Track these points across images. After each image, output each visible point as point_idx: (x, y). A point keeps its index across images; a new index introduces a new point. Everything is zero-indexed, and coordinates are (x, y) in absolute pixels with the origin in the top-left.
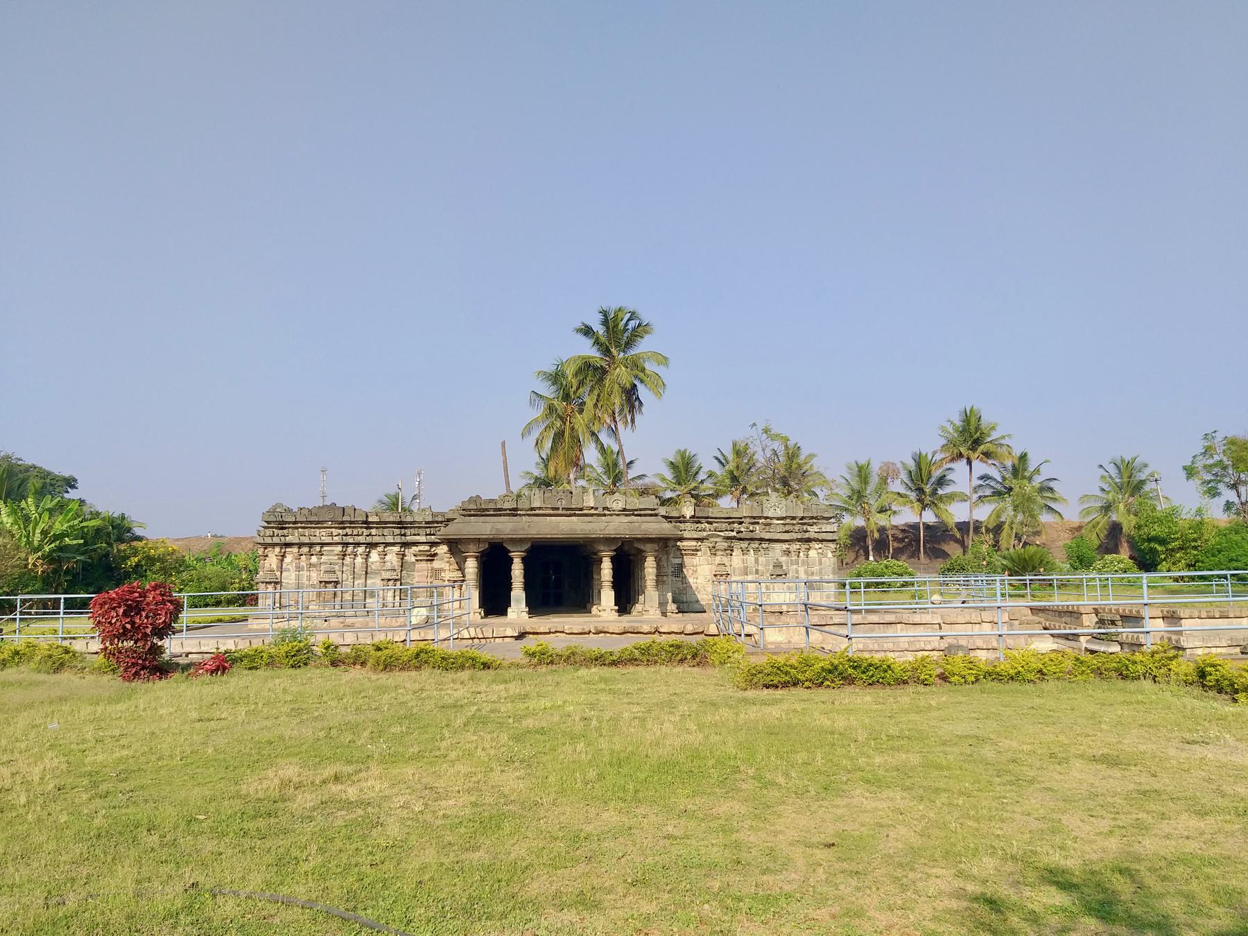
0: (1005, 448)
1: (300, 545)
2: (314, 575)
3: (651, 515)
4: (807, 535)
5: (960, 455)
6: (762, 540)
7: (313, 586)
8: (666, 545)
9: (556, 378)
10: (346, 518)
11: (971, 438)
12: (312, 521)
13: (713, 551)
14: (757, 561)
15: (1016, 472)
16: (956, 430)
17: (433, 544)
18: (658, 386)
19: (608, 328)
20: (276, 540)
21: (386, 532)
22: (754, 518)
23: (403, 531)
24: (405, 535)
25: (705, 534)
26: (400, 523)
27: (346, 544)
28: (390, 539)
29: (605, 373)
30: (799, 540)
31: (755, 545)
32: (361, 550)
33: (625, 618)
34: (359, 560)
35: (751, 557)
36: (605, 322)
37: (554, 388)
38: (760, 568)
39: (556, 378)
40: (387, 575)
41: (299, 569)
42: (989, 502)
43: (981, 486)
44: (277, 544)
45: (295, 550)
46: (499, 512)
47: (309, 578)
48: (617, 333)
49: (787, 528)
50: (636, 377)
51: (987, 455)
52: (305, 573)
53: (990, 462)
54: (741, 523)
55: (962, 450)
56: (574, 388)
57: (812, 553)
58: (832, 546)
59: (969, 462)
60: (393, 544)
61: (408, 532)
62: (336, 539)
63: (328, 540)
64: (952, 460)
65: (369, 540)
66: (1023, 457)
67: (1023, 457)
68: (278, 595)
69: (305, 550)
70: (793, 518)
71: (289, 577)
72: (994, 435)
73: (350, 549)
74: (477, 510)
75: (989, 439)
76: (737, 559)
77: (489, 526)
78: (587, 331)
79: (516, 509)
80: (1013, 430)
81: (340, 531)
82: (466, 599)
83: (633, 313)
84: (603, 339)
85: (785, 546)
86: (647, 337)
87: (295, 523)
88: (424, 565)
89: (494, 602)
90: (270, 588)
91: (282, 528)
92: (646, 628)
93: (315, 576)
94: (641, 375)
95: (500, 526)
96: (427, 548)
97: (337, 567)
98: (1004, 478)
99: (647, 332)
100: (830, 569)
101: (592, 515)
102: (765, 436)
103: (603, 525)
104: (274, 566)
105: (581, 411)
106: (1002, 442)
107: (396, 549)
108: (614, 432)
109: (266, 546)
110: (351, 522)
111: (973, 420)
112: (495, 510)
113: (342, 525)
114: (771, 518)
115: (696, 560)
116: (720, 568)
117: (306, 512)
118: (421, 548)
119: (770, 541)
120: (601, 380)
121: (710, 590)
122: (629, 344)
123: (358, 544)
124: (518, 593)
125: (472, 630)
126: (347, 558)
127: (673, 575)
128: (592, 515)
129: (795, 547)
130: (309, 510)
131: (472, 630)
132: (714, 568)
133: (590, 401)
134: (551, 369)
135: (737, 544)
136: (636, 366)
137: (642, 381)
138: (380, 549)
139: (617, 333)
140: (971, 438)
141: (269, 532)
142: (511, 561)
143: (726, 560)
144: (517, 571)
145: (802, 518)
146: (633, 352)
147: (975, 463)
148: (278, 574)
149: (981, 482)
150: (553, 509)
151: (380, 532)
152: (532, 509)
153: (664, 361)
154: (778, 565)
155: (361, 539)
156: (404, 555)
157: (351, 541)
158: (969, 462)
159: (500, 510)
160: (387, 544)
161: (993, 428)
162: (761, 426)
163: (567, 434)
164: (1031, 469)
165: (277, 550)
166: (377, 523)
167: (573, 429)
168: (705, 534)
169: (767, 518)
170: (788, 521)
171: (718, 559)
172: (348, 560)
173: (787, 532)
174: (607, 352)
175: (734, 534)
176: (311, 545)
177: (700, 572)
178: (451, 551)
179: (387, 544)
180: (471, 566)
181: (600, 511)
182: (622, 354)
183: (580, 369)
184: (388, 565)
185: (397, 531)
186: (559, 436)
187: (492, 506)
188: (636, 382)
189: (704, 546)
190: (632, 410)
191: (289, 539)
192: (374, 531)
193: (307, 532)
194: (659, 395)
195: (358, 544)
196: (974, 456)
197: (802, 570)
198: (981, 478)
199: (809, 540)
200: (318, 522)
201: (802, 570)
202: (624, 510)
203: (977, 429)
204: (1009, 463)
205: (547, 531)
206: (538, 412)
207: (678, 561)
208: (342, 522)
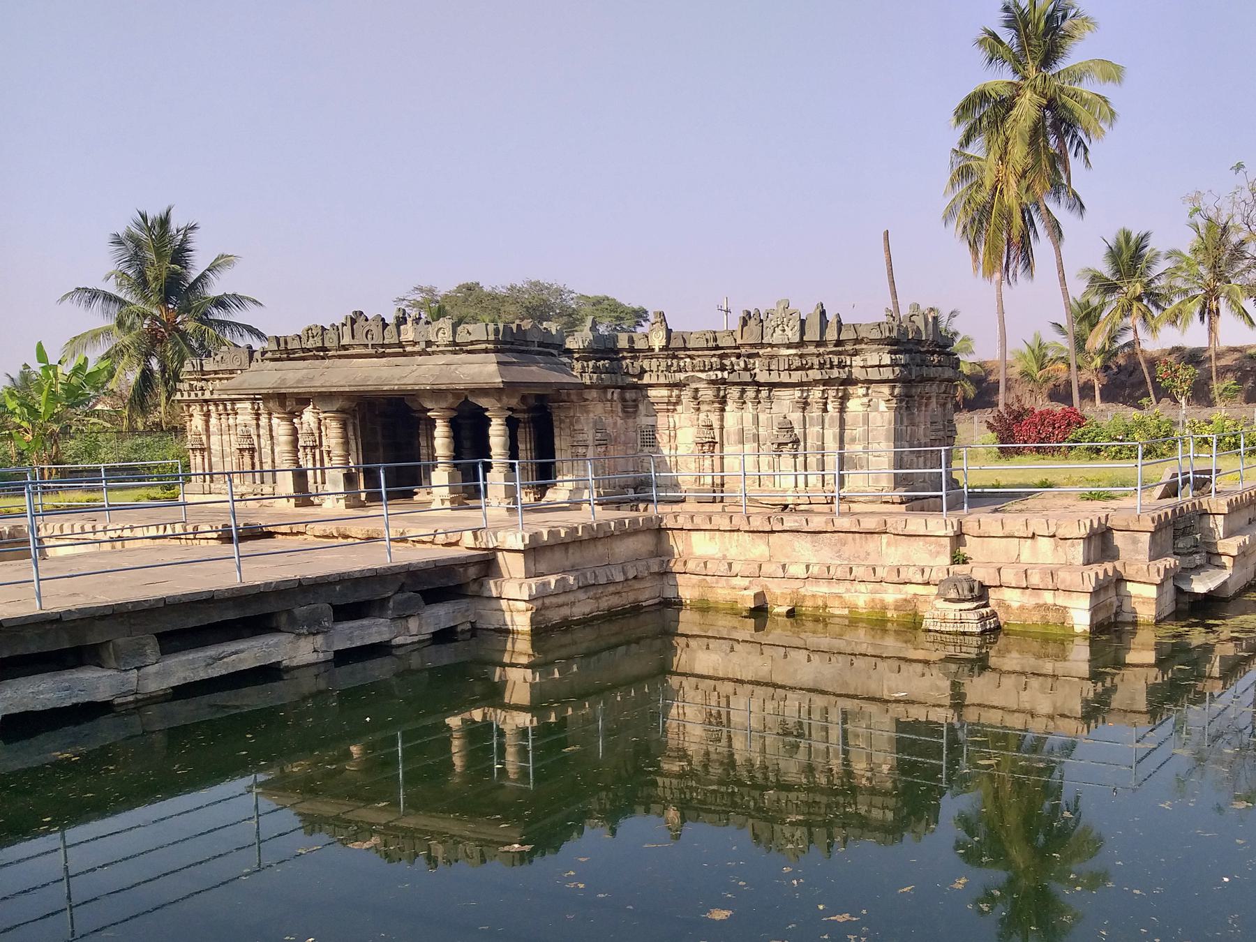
52: (225, 437)
101: (412, 354)
104: (200, 428)
128: (412, 354)
148: (204, 438)
191: (207, 396)
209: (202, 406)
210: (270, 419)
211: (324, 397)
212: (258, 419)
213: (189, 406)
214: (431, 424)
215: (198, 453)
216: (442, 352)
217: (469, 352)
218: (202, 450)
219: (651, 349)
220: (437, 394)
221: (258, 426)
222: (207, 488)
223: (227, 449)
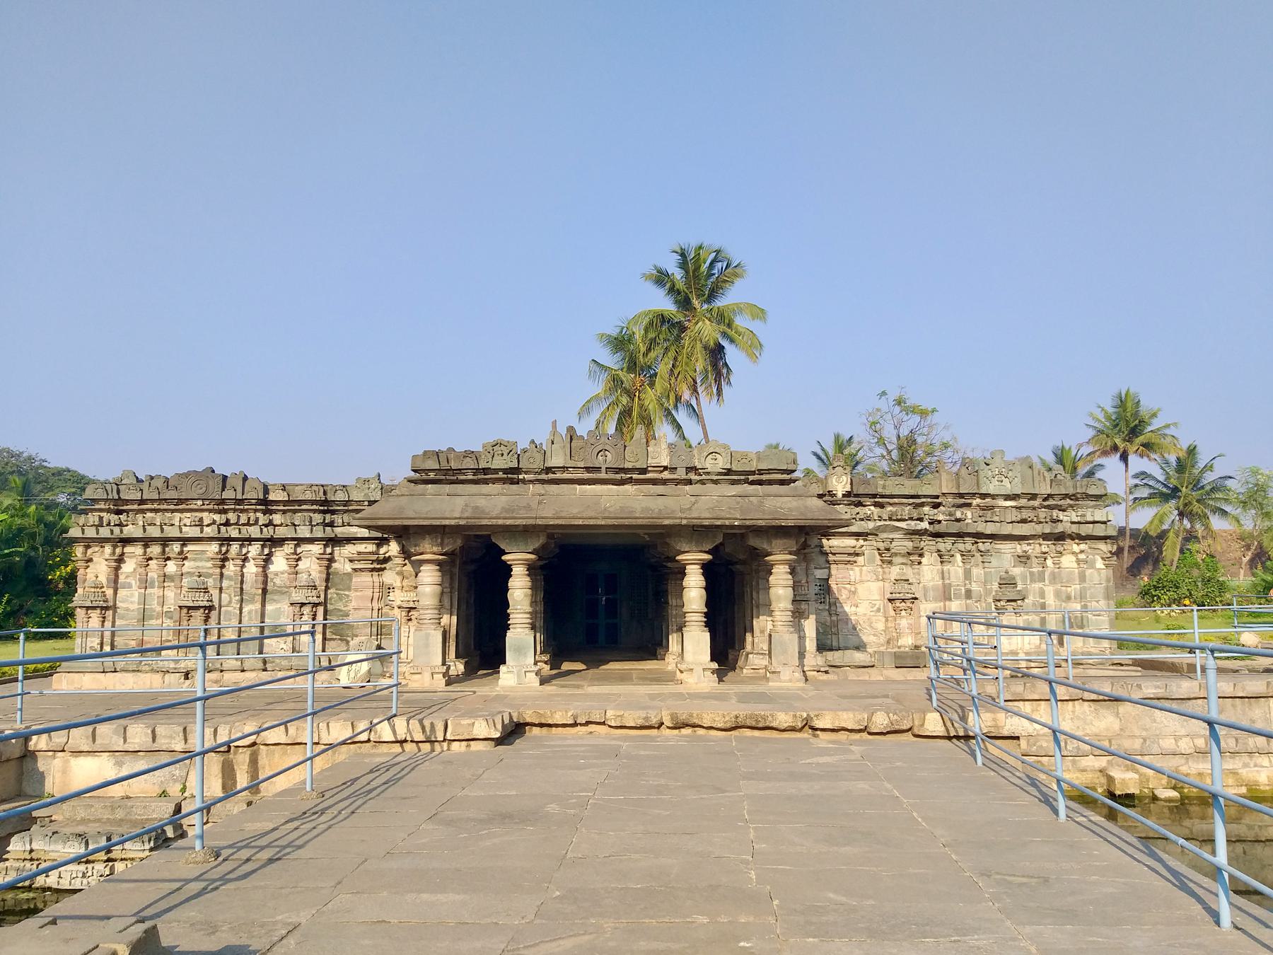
0: (1169, 439)
1: (147, 542)
3: (782, 482)
4: (1060, 528)
5: (1115, 448)
6: (978, 536)
7: (169, 615)
8: (807, 539)
9: (620, 343)
10: (228, 494)
11: (1128, 428)
12: (169, 495)
13: (887, 557)
14: (968, 575)
15: (1181, 467)
16: (1108, 418)
18: (754, 347)
19: (687, 272)
20: (104, 532)
21: (298, 518)
22: (961, 496)
23: (328, 518)
24: (331, 524)
25: (871, 525)
26: (325, 502)
28: (304, 532)
29: (685, 328)
30: (1046, 537)
31: (968, 544)
32: (254, 550)
33: (730, 687)
34: (251, 569)
35: (956, 568)
36: (683, 265)
37: (618, 356)
38: (975, 587)
39: (620, 343)
40: (299, 597)
41: (145, 584)
42: (1150, 505)
43: (1136, 486)
44: (106, 540)
45: (137, 550)
46: (483, 475)
48: (698, 279)
49: (1026, 514)
50: (724, 335)
51: (1147, 446)
52: (155, 592)
53: (1153, 456)
54: (936, 506)
55: (1118, 441)
56: (643, 349)
57: (1068, 561)
58: (1104, 547)
59: (1124, 458)
60: (311, 541)
61: (338, 519)
62: (209, 532)
64: (1105, 453)
65: (268, 532)
66: (1192, 451)
67: (1192, 451)
69: (155, 550)
70: (1033, 497)
71: (129, 599)
72: (1156, 424)
73: (235, 547)
74: (440, 472)
75: (1150, 428)
76: (929, 571)
77: (460, 502)
78: (661, 278)
79: (517, 470)
80: (1181, 419)
81: (217, 517)
82: (425, 649)
83: (718, 252)
84: (680, 285)
85: (1019, 548)
86: (738, 282)
88: (366, 578)
89: (481, 647)
90: (95, 615)
91: (119, 512)
92: (783, 719)
94: (732, 333)
95: (482, 502)
96: (371, 547)
97: (210, 582)
98: (1168, 478)
99: (736, 275)
100: (1100, 590)
101: (664, 482)
102: (897, 409)
103: (686, 501)
104: (103, 579)
105: (652, 385)
106: (1167, 431)
107: (316, 549)
108: (695, 413)
111: (1129, 405)
112: (477, 471)
113: (220, 506)
114: (993, 497)
115: (854, 573)
116: (898, 587)
117: (159, 483)
118: (362, 547)
119: (993, 537)
120: (678, 339)
121: (880, 626)
122: (712, 296)
123: (250, 540)
124: (521, 636)
125: (400, 723)
127: (817, 597)
128: (664, 482)
129: (1034, 548)
130: (167, 481)
131: (400, 723)
132: (889, 587)
133: (663, 369)
134: (614, 332)
135: (927, 544)
136: (723, 319)
137: (732, 341)
138: (288, 548)
139: (698, 279)
140: (1128, 428)
142: (507, 571)
143: (909, 572)
144: (519, 590)
145: (1050, 496)
146: (720, 303)
147: (1132, 458)
148: (110, 592)
149: (1137, 481)
150: (588, 469)
151: (287, 518)
152: (548, 470)
153: (759, 313)
154: (1008, 582)
155: (254, 532)
156: (331, 560)
157: (235, 534)
158: (1124, 458)
159: (486, 471)
160: (300, 541)
161: (1154, 415)
162: (893, 395)
163: (635, 414)
164: (1201, 465)
165: (108, 549)
166: (285, 503)
167: (641, 406)
168: (871, 525)
169: (984, 496)
170: (1023, 502)
171: (895, 571)
172: (231, 568)
173: (1024, 521)
174: (684, 303)
175: (925, 525)
176: (165, 542)
177: (861, 588)
178: (406, 554)
179: (300, 541)
180: (430, 577)
181: (681, 474)
182: (706, 306)
183: (651, 323)
184: (303, 578)
185: (318, 518)
186: (626, 413)
187: (469, 463)
188: (724, 343)
189: (868, 547)
190: (718, 378)
191: (130, 531)
192: (277, 519)
193: (158, 518)
194: (753, 357)
195: (250, 540)
196: (1132, 448)
197: (1050, 591)
198: (1136, 476)
199: (1060, 537)
201: (1050, 591)
202: (729, 472)
203: (1136, 415)
204: (1172, 459)
205: (575, 511)
206: (598, 387)
207: (820, 574)
209: (115, 547)
210: (243, 566)
211: (437, 531)
212: (223, 567)
213: (88, 547)
214: (682, 573)
215: (95, 615)
216: (716, 482)
217: (752, 483)
218: (107, 608)
219: (831, 494)
220: (697, 532)
221: (222, 575)
223: (154, 605)
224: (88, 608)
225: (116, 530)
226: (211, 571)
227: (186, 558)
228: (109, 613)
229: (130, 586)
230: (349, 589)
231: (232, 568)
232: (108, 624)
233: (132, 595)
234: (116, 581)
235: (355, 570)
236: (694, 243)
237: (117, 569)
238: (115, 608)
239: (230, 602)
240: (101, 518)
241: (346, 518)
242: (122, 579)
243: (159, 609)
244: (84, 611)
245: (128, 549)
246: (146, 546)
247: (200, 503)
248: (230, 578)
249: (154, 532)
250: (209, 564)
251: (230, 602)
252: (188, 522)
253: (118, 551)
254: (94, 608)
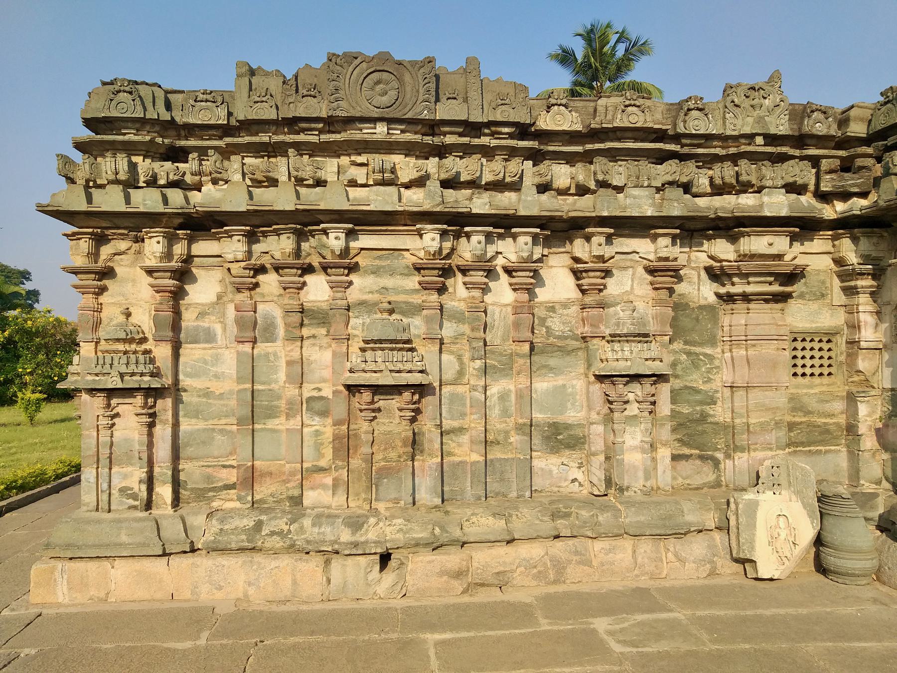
1: (257, 223)
2: (321, 356)
7: (318, 406)
17: (803, 227)
20: (146, 200)
21: (619, 173)
27: (456, 223)
41: (251, 331)
44: (151, 219)
45: (233, 247)
47: (299, 372)
52: (278, 351)
62: (416, 199)
63: (380, 199)
68: (162, 451)
69: (279, 246)
71: (212, 367)
78: (565, 58)
86: (644, 59)
87: (226, 130)
88: (762, 316)
90: (130, 413)
91: (177, 155)
93: (326, 364)
97: (417, 326)
104: (143, 319)
109: (98, 226)
110: (472, 128)
113: (429, 137)
126: (457, 284)
141: (112, 165)
148: (162, 352)
157: (481, 204)
165: (154, 246)
166: (572, 137)
176: (305, 222)
191: (208, 198)
200: (331, 123)
208: (433, 127)
209: (171, 239)
213: (100, 240)
215: (130, 413)
222: (173, 530)
224: (111, 393)
225: (176, 196)
226: (417, 299)
227: (353, 268)
228: (165, 405)
229: (209, 337)
230: (712, 341)
231: (462, 292)
232: (163, 432)
233: (217, 359)
234: (176, 326)
235: (729, 298)
236: (604, 21)
237: (178, 295)
238: (175, 390)
239: (461, 373)
240: (133, 167)
241: (726, 172)
242: (189, 319)
243: (292, 391)
244: (99, 401)
245: (202, 247)
246: (252, 238)
247: (381, 130)
248: (458, 317)
249: (282, 199)
250: (413, 282)
251: (461, 373)
252: (360, 175)
253: (179, 249)
254: (127, 392)
